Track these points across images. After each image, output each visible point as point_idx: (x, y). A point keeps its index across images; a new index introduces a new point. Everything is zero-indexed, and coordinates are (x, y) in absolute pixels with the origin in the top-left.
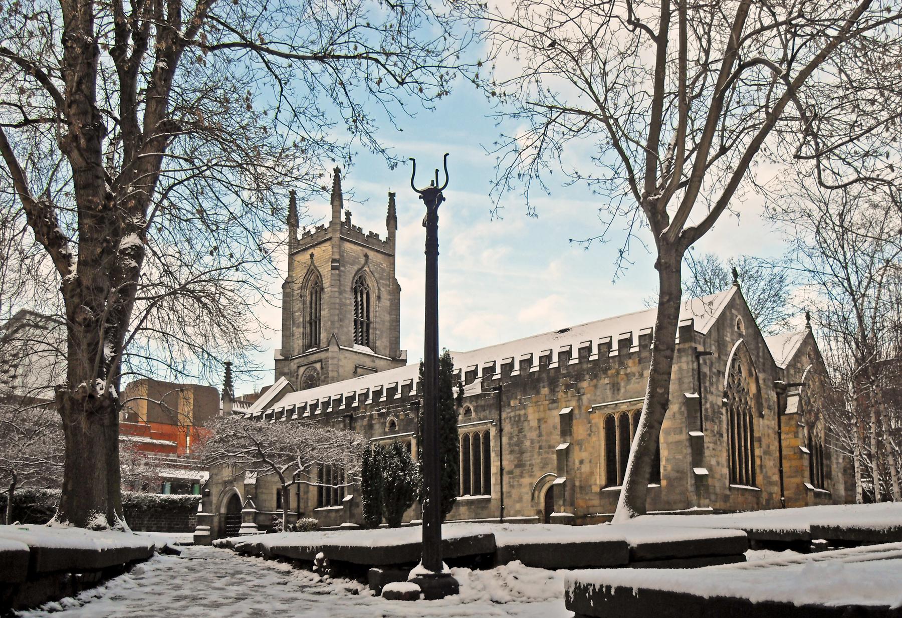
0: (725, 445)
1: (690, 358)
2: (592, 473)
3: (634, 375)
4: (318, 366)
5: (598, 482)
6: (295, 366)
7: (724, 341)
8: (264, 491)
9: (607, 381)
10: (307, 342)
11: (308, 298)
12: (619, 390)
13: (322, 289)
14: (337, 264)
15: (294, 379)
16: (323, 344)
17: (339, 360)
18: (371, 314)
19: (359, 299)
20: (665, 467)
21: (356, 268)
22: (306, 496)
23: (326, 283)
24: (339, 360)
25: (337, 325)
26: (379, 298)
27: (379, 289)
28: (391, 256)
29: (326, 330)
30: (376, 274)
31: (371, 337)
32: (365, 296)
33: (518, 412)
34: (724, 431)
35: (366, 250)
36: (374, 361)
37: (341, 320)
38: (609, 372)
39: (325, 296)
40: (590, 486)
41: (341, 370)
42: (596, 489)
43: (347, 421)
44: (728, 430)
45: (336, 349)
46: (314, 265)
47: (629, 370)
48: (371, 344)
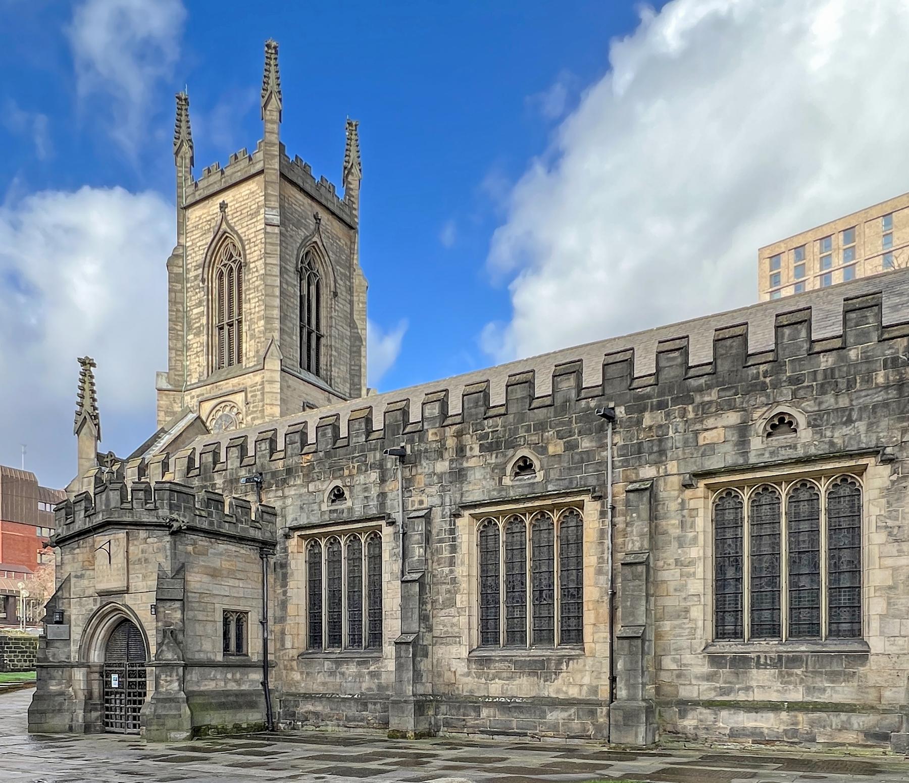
8: (201, 616)
11: (216, 284)
22: (278, 628)
30: (330, 254)
32: (313, 288)
35: (317, 208)
46: (227, 223)
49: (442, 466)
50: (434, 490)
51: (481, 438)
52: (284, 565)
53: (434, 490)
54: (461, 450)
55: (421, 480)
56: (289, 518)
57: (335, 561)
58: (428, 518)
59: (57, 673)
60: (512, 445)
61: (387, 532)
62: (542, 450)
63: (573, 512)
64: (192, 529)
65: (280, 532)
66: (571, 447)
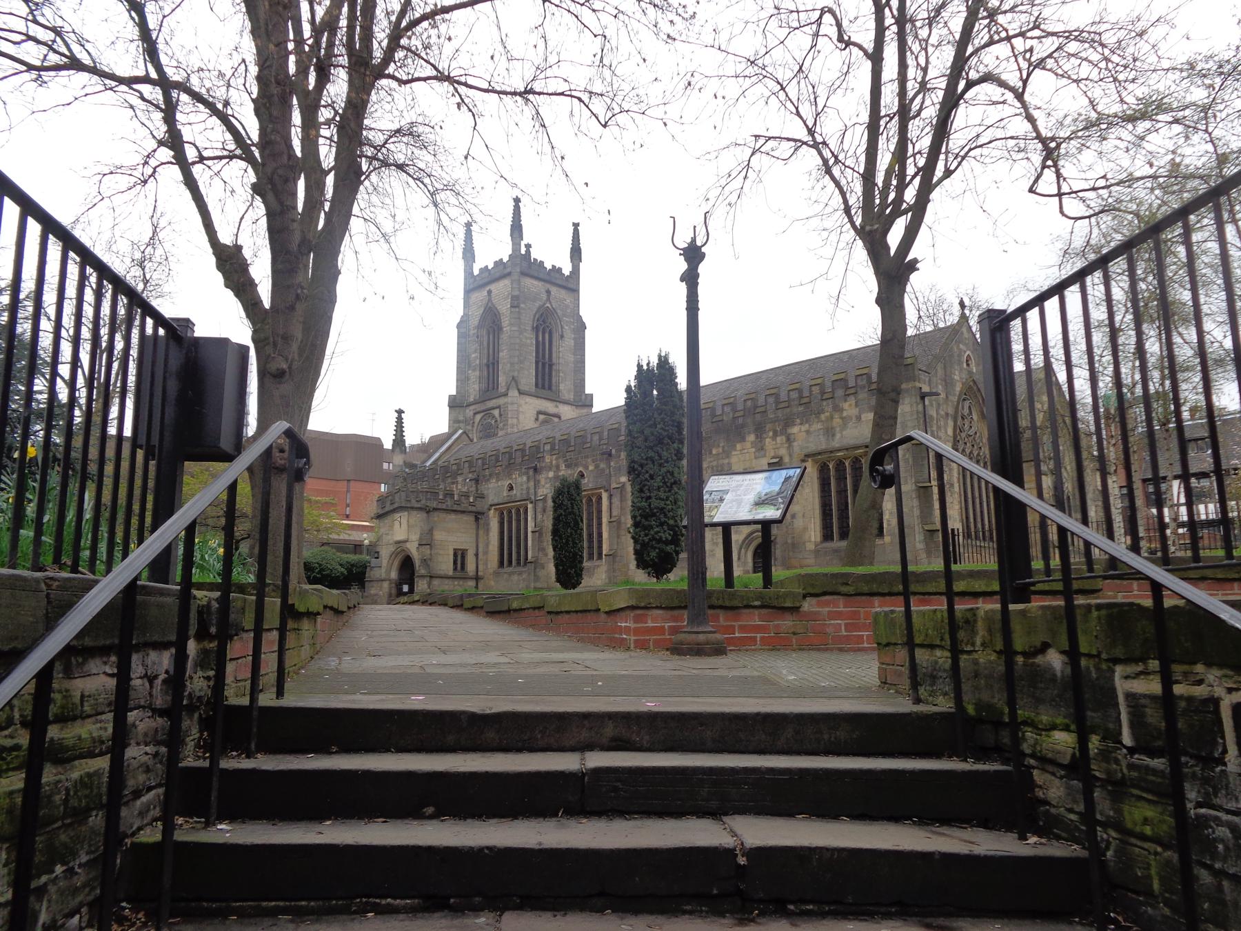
0: (956, 496)
1: (914, 400)
2: (805, 529)
3: (850, 418)
4: (496, 412)
5: (813, 539)
6: (472, 413)
7: (953, 379)
8: (441, 552)
9: (819, 426)
10: (484, 386)
11: (486, 339)
12: (834, 435)
13: (500, 329)
14: (516, 302)
15: (469, 427)
16: (502, 389)
17: (520, 406)
18: (554, 355)
19: (541, 339)
20: (888, 521)
21: (537, 305)
23: (505, 322)
24: (520, 406)
25: (516, 367)
26: (562, 336)
27: (562, 327)
28: (575, 291)
29: (504, 373)
31: (554, 380)
33: (721, 462)
34: (955, 480)
36: (557, 407)
37: (521, 362)
38: (823, 417)
39: (504, 337)
40: (804, 543)
41: (521, 417)
42: (811, 546)
43: (531, 472)
44: (959, 479)
45: (516, 393)
47: (845, 414)
48: (554, 388)
49: (551, 474)
50: (548, 486)
51: (567, 461)
52: (488, 525)
53: (548, 486)
54: (558, 467)
55: (543, 482)
56: (490, 499)
57: (510, 522)
58: (544, 500)
59: (375, 584)
60: (576, 465)
61: (530, 506)
62: (586, 468)
63: (600, 498)
64: (435, 509)
65: (486, 507)
66: (597, 467)
